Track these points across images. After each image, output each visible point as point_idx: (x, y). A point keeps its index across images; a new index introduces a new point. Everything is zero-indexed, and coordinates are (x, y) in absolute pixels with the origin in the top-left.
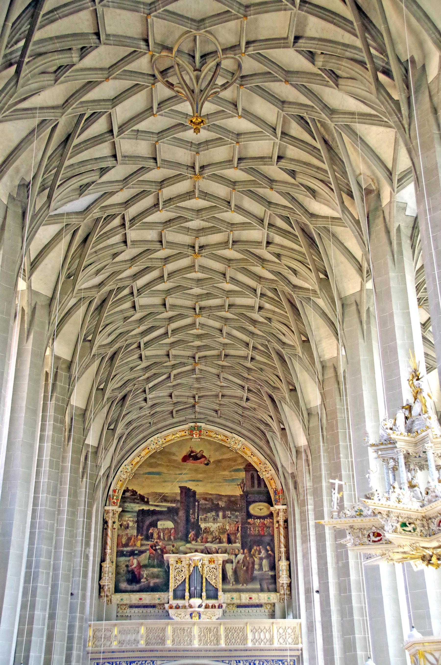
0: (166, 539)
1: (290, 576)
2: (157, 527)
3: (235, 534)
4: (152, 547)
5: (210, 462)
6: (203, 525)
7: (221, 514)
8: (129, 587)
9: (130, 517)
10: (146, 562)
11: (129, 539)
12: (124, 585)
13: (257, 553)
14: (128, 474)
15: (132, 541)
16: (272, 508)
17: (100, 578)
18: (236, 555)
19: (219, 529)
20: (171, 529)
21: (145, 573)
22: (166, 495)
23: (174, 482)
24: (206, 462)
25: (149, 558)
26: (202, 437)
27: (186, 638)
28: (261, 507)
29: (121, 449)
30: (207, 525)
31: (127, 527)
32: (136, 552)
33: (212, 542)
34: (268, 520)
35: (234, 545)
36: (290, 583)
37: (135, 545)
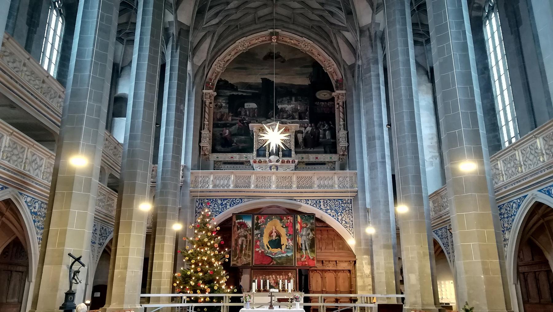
0: (251, 116)
1: (348, 142)
2: (244, 107)
3: (305, 113)
4: (240, 121)
5: (285, 60)
6: (280, 107)
7: (293, 99)
8: (223, 149)
9: (222, 100)
10: (236, 132)
11: (222, 115)
12: (219, 148)
13: (322, 126)
14: (221, 68)
15: (225, 117)
16: (334, 94)
17: (200, 141)
18: (305, 128)
19: (292, 109)
20: (255, 109)
21: (235, 140)
22: (251, 84)
23: (257, 75)
24: (282, 61)
25: (238, 130)
26: (279, 42)
27: (267, 183)
28: (325, 94)
29: (215, 47)
30: (283, 106)
31: (221, 107)
32: (228, 125)
33: (286, 118)
34: (331, 103)
35: (304, 120)
36: (348, 146)
37: (227, 120)
